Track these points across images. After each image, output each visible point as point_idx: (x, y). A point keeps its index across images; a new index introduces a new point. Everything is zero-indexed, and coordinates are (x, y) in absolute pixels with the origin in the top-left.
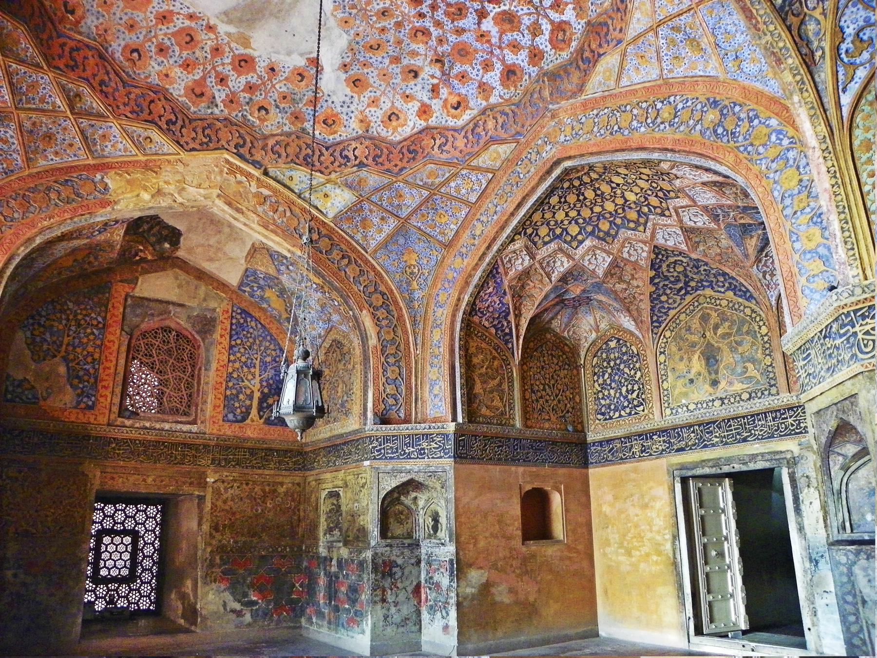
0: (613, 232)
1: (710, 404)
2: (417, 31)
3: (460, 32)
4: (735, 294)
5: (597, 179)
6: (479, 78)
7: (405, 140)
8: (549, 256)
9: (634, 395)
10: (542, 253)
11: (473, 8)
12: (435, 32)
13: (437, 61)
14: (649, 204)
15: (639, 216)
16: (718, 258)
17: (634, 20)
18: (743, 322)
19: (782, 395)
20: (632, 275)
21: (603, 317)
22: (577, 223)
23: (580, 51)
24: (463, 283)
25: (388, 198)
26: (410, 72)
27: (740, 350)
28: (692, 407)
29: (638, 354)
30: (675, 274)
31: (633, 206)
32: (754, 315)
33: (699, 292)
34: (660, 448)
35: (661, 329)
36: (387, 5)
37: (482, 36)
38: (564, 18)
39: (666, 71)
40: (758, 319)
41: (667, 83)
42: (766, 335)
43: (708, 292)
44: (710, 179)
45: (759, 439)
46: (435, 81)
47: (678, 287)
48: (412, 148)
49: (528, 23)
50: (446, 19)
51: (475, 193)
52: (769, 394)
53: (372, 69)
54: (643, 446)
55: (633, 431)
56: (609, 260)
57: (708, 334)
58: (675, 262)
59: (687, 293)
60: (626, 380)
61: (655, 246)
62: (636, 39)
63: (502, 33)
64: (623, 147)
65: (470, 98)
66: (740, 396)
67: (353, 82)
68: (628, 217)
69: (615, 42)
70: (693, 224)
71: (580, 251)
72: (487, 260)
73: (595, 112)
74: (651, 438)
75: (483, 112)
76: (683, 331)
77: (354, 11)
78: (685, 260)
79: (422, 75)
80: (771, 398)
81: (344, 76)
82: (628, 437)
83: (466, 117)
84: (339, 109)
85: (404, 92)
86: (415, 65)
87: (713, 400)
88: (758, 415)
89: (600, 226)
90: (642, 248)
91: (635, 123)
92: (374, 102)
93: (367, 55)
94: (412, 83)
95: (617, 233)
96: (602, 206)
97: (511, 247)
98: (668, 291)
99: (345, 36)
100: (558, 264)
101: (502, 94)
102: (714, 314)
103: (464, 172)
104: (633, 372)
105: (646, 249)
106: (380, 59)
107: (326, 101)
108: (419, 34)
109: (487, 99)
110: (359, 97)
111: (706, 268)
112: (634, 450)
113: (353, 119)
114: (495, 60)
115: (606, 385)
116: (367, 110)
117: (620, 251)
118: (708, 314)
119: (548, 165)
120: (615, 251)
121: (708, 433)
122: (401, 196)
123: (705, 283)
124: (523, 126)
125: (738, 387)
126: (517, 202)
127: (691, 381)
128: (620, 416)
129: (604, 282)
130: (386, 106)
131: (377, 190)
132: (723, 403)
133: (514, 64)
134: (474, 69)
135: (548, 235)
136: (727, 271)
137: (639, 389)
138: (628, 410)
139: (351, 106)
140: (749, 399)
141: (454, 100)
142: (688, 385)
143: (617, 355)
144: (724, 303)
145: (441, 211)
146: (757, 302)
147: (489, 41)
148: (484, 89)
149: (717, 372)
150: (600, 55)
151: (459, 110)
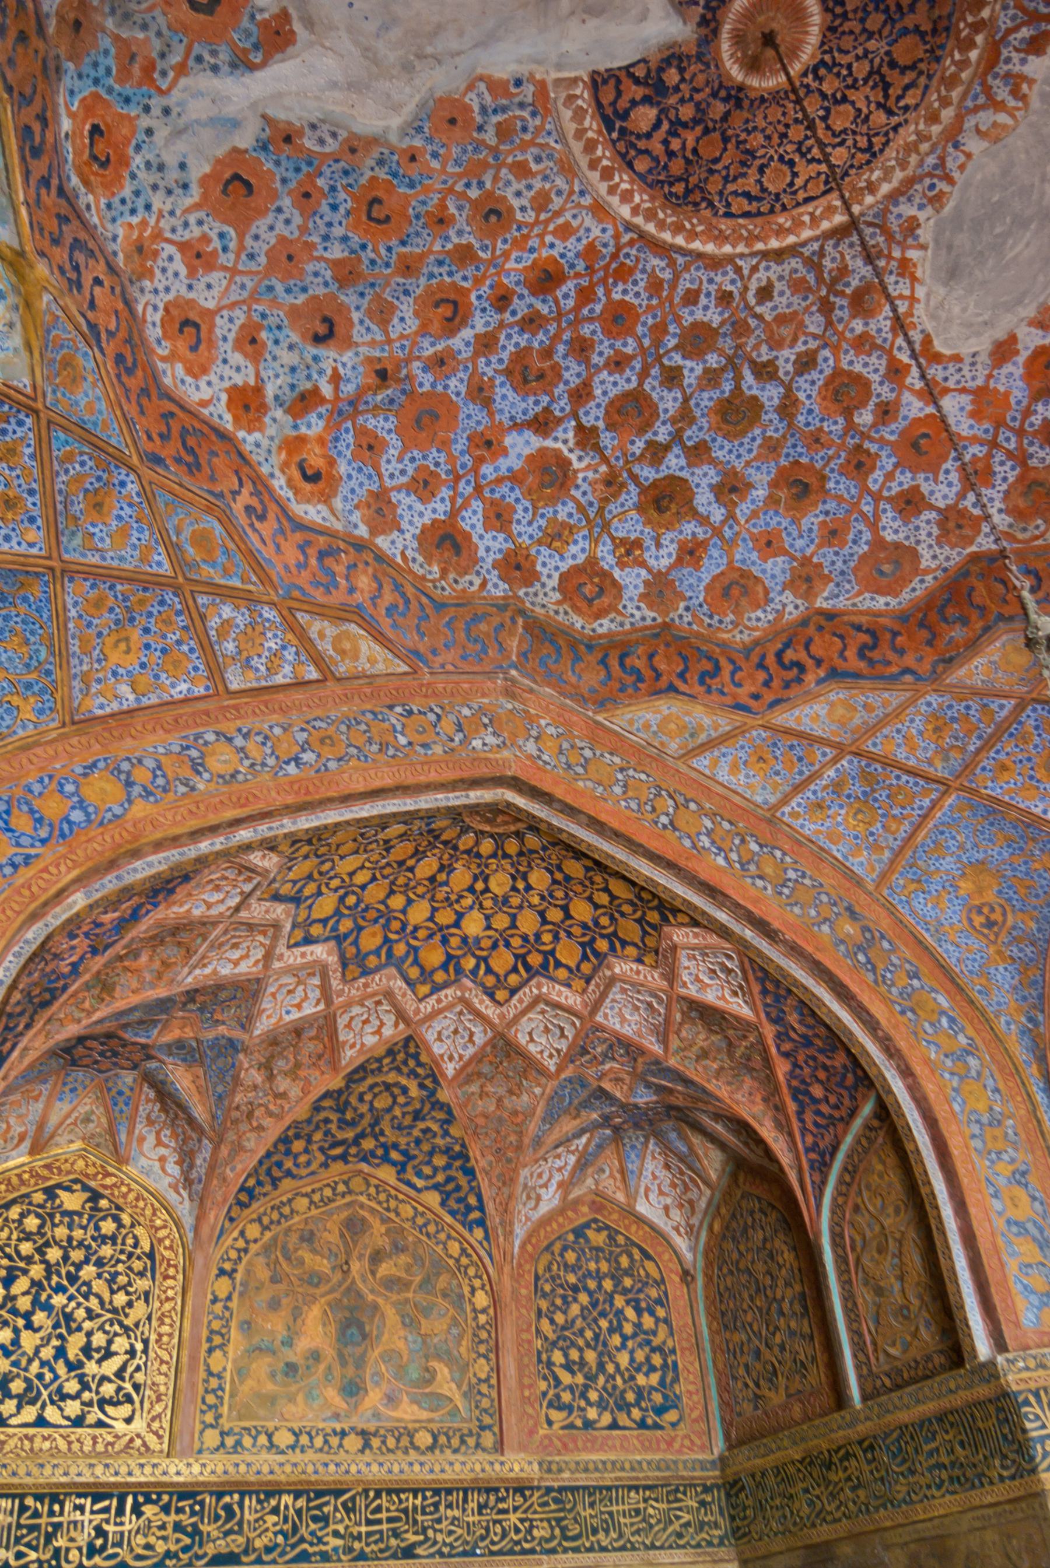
0: (372, 961)
1: (335, 1441)
2: (455, 303)
3: (480, 393)
4: (443, 1204)
5: (478, 855)
6: (388, 483)
7: (182, 407)
8: (250, 927)
9: (110, 1367)
10: (258, 911)
11: (553, 400)
12: (462, 340)
13: (383, 375)
14: (485, 959)
15: (444, 966)
16: (481, 1121)
17: (807, 710)
18: (438, 1267)
19: (509, 1456)
20: (298, 1065)
21: (87, 1120)
22: (342, 899)
23: (618, 648)
24: (109, 855)
25: (78, 479)
26: (326, 320)
27: (425, 1326)
28: (283, 1439)
29: (151, 1256)
30: (364, 1108)
31: (454, 941)
32: (464, 1261)
33: (364, 1167)
34: (161, 1547)
35: (246, 1212)
36: (519, 216)
37: (489, 444)
38: (617, 573)
39: (787, 809)
40: (471, 1272)
41: (772, 821)
42: (484, 1311)
43: (387, 1174)
44: (720, 1004)
45: (442, 1554)
46: (327, 390)
47: (340, 1136)
48: (190, 445)
49: (562, 516)
50: (505, 355)
51: (251, 675)
52: (478, 1445)
53: (297, 220)
54: (100, 1532)
55: (87, 1478)
56: (309, 1010)
57: (355, 1266)
58: (388, 1087)
59: (344, 1158)
60: (91, 1315)
61: (409, 1039)
62: (788, 732)
63: (515, 478)
64: (682, 863)
65: (344, 490)
66: (411, 1436)
67: (236, 177)
68: (422, 954)
69: (728, 700)
70: (523, 1039)
71: (294, 957)
72: (204, 846)
73: (617, 760)
74: (137, 1511)
75: (360, 546)
76: (294, 1238)
77: (490, 137)
78: (414, 1091)
79: (329, 356)
80: (480, 1455)
81: (245, 140)
82: (54, 1497)
83: (313, 513)
84: (138, 160)
85: (259, 327)
86: (352, 324)
87: (343, 1434)
88: (449, 1492)
89: (364, 934)
90: (382, 1024)
91: (705, 841)
92: (198, 257)
93: (342, 195)
94: (295, 338)
95: (377, 969)
96: (410, 901)
97: (256, 858)
98: (318, 1136)
99: (395, 122)
100: (236, 955)
101: (409, 553)
102: (378, 1228)
103: (268, 613)
104: (120, 1299)
105: (388, 1031)
106: (338, 231)
107: (147, 109)
108: (446, 310)
109: (374, 532)
110: (197, 206)
111: (435, 1127)
112: (60, 1542)
113: (135, 220)
114: (445, 492)
115: (14, 1312)
116: (170, 249)
117: (349, 1005)
118: (363, 1220)
119: (484, 771)
120: (338, 1001)
121: (315, 1519)
122: (98, 506)
123: (394, 1155)
124: (434, 652)
125: (408, 1412)
126: (377, 784)
127: (291, 1368)
128: (41, 1421)
129: (245, 1050)
130: (208, 293)
131: (83, 432)
132: (367, 1445)
133: (468, 536)
134: (400, 460)
135: (295, 882)
136: (474, 1152)
137: (132, 1352)
138: (73, 1408)
139: (161, 193)
140: (431, 1449)
141: (316, 461)
142: (279, 1377)
143: (78, 1234)
144: (407, 1211)
145: (136, 635)
146: (487, 1237)
147: (480, 460)
148: (381, 511)
149: (360, 1363)
150: (672, 688)
151: (308, 487)
